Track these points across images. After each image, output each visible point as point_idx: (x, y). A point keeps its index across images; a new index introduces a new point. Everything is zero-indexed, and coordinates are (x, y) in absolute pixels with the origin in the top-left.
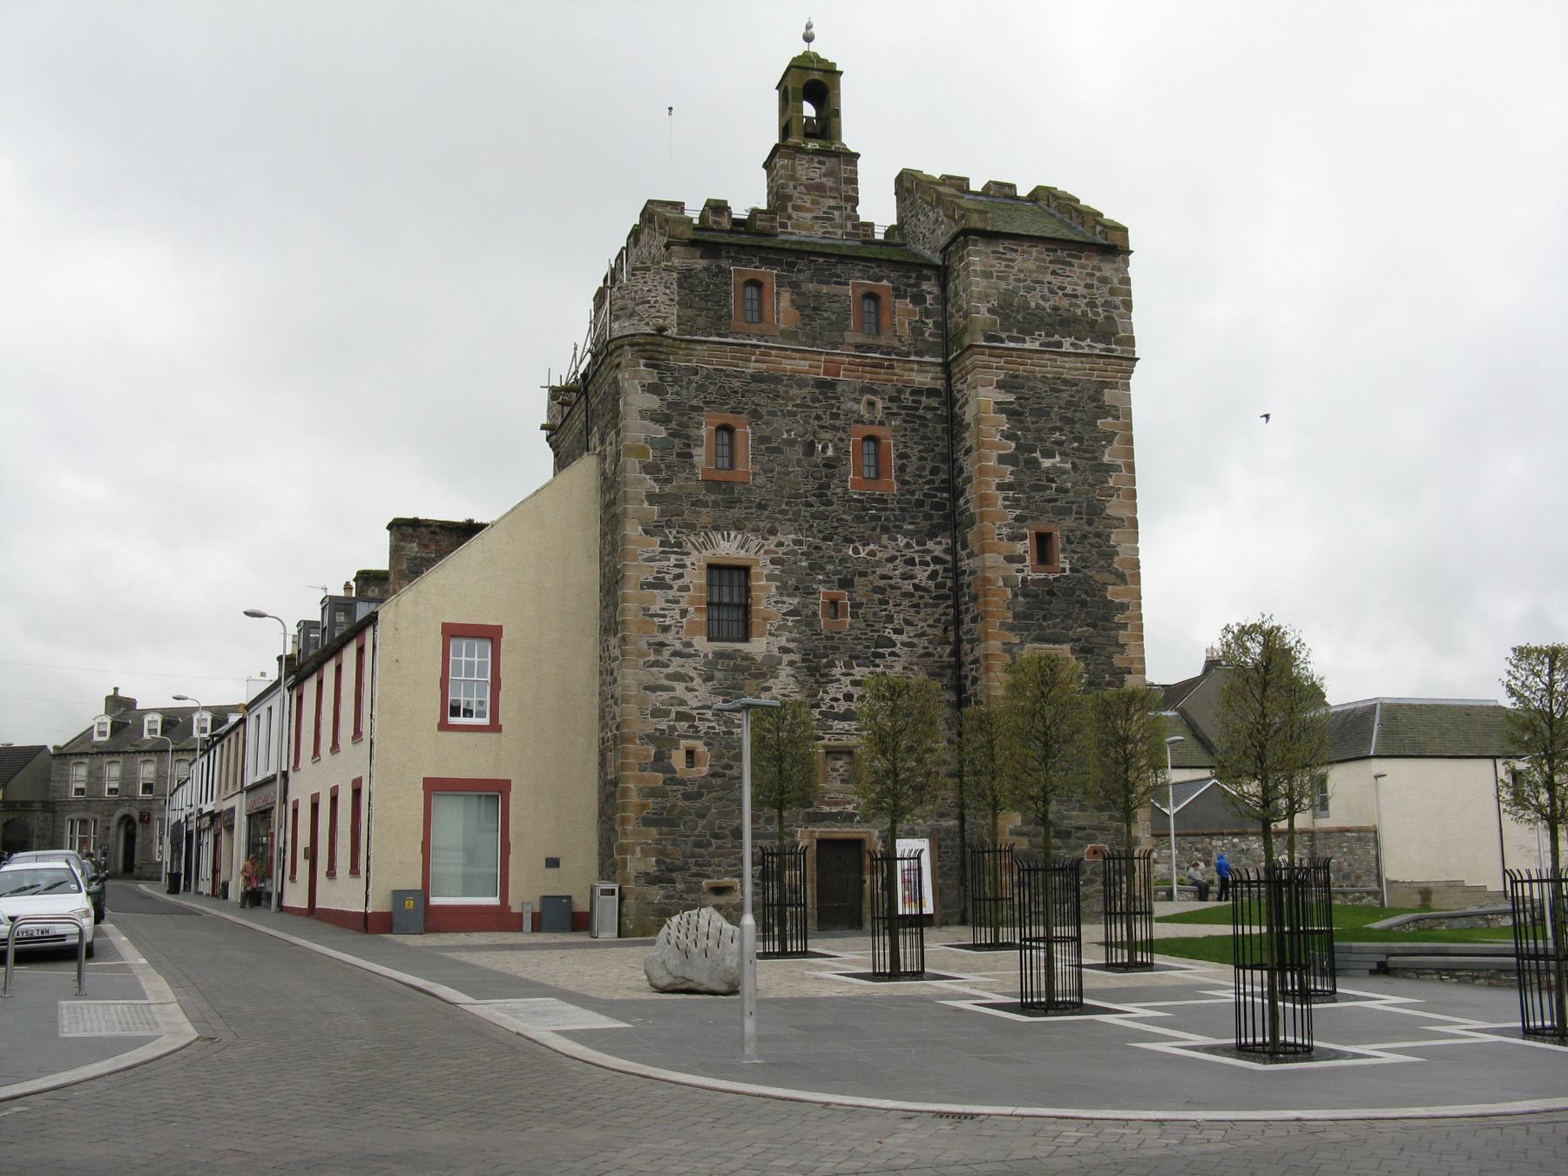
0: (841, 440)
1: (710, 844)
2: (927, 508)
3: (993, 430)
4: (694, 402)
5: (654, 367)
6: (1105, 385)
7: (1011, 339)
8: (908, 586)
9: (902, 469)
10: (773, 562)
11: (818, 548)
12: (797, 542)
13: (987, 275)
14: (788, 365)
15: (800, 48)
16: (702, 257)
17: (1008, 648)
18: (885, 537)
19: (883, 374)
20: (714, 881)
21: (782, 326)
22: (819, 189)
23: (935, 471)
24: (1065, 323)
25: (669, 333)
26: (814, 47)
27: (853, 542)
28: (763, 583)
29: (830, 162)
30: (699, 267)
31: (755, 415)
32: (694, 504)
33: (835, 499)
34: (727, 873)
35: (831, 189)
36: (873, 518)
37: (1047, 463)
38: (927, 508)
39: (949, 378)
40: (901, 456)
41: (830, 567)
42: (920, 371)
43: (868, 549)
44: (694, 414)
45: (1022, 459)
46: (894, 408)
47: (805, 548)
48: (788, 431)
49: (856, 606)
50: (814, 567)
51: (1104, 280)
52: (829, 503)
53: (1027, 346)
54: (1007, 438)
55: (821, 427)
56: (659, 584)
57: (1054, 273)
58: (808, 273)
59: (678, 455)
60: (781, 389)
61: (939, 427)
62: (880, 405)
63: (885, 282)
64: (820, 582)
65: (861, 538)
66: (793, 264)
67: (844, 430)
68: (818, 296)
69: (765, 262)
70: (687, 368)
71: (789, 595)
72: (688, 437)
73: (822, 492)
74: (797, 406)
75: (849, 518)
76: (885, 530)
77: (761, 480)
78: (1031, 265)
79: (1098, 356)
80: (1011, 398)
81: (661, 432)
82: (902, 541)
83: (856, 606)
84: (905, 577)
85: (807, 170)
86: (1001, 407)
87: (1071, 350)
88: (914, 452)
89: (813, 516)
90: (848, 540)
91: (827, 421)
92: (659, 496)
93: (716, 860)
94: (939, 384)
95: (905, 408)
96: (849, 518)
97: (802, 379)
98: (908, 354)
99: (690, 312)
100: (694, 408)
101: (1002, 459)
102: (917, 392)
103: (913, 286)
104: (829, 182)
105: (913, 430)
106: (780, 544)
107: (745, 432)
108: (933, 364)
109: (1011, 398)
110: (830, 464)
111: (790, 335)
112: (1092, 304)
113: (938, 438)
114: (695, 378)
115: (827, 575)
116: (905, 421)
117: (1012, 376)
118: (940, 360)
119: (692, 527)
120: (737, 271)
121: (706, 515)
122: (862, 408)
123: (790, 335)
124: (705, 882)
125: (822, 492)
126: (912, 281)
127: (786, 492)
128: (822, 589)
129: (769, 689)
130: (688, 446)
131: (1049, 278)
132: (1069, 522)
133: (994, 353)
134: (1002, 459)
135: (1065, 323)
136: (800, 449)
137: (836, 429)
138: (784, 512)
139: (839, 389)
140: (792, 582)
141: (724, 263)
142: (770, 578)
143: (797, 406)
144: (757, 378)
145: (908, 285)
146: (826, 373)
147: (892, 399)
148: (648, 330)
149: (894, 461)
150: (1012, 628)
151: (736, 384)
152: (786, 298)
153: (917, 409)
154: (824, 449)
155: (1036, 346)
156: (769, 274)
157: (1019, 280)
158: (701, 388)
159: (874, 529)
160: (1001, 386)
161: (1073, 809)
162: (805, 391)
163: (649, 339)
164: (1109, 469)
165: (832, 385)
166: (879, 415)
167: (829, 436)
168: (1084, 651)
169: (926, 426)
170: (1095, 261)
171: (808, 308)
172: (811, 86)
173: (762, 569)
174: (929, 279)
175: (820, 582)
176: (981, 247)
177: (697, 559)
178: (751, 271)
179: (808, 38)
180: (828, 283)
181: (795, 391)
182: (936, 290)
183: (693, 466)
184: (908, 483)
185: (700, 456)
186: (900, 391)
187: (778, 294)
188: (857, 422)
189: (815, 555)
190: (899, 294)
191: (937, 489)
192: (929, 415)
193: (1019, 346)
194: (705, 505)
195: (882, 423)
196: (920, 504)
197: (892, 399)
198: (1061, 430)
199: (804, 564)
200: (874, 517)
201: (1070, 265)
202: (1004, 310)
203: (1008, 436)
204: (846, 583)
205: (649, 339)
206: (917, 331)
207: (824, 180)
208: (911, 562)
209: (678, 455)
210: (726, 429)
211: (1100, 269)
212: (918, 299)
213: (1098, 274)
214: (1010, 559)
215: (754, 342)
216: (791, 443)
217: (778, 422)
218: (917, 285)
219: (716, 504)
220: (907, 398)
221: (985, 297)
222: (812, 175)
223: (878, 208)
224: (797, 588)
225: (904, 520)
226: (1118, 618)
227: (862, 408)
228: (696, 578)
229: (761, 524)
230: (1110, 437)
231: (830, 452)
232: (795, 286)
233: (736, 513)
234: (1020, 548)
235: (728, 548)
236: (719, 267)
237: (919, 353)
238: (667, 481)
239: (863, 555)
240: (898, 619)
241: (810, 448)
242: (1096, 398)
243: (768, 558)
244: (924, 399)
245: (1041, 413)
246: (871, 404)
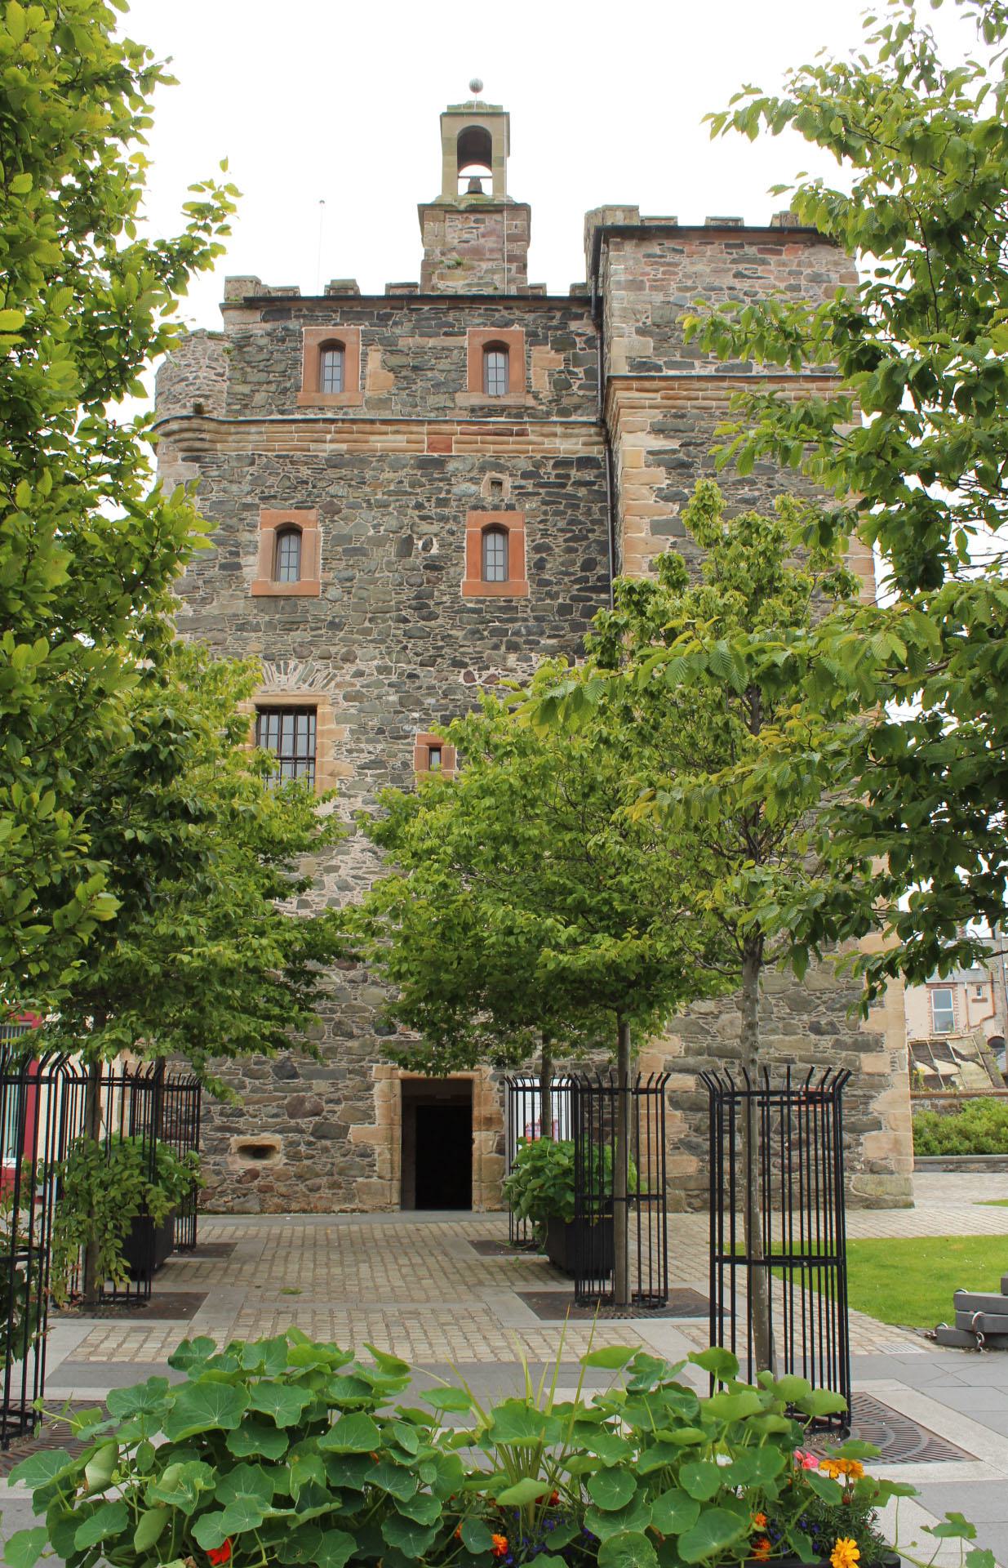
0: (452, 533)
1: (242, 1086)
2: (576, 615)
3: (645, 490)
4: (249, 500)
5: (196, 459)
7: (672, 365)
9: (540, 565)
10: (346, 698)
11: (412, 676)
12: (381, 670)
13: (635, 285)
14: (378, 443)
15: (463, 97)
16: (264, 320)
18: (512, 659)
19: (511, 444)
20: (248, 1139)
21: (368, 394)
23: (589, 565)
25: (214, 415)
26: (487, 98)
27: (464, 665)
28: (333, 726)
29: (490, 221)
30: (260, 332)
31: (331, 511)
32: (241, 628)
33: (439, 610)
34: (264, 1128)
35: (492, 250)
36: (495, 632)
38: (576, 615)
39: (608, 440)
40: (538, 549)
41: (432, 701)
42: (565, 436)
43: (486, 674)
44: (245, 514)
46: (529, 485)
47: (394, 678)
48: (374, 527)
51: (816, 279)
52: (432, 616)
53: (698, 371)
54: (666, 499)
55: (422, 518)
57: (738, 275)
58: (411, 325)
59: (223, 567)
60: (368, 474)
61: (596, 508)
62: (508, 482)
63: (516, 327)
64: (415, 721)
65: (478, 659)
66: (389, 316)
67: (455, 518)
68: (420, 352)
70: (239, 458)
71: (368, 741)
72: (238, 545)
73: (421, 606)
74: (389, 493)
75: (460, 634)
76: (513, 647)
77: (333, 592)
78: (700, 267)
79: (806, 378)
80: (674, 444)
82: (538, 660)
85: (455, 231)
87: (766, 373)
88: (558, 543)
89: (409, 635)
90: (458, 664)
91: (432, 510)
92: (192, 620)
93: (251, 1108)
94: (596, 451)
95: (543, 485)
96: (460, 634)
97: (397, 459)
98: (548, 414)
99: (246, 389)
100: (247, 507)
102: (559, 464)
103: (556, 328)
104: (490, 243)
105: (556, 513)
106: (359, 674)
107: (314, 529)
108: (584, 424)
109: (674, 444)
110: (433, 566)
113: (593, 522)
114: (251, 469)
115: (426, 711)
116: (545, 503)
117: (675, 416)
118: (593, 419)
120: (314, 333)
121: (255, 643)
122: (483, 490)
123: (383, 403)
124: (235, 1140)
125: (421, 606)
126: (555, 323)
127: (373, 605)
128: (417, 730)
129: (336, 869)
130: (237, 554)
131: (729, 280)
134: (657, 528)
136: (392, 549)
137: (443, 519)
138: (366, 632)
139: (451, 466)
140: (374, 723)
141: (293, 324)
142: (341, 719)
143: (389, 493)
145: (549, 328)
146: (431, 448)
147: (526, 475)
148: (185, 413)
149: (528, 557)
151: (305, 472)
152: (375, 357)
153: (563, 486)
154: (427, 547)
155: (710, 370)
156: (351, 332)
157: (687, 289)
158: (256, 481)
159: (496, 647)
160: (658, 430)
161: (774, 1031)
162: (402, 473)
163: (185, 424)
165: (440, 463)
166: (507, 494)
167: (435, 528)
169: (576, 507)
170: (804, 254)
171: (408, 372)
174: (579, 317)
175: (415, 721)
176: (629, 248)
178: (327, 331)
179: (476, 88)
180: (437, 335)
181: (388, 475)
182: (590, 331)
183: (240, 580)
184: (548, 583)
185: (253, 567)
186: (538, 465)
187: (365, 354)
188: (475, 508)
189: (409, 685)
190: (533, 338)
191: (594, 589)
192: (582, 492)
193: (685, 373)
194: (256, 629)
195: (510, 507)
196: (564, 610)
197: (526, 475)
198: (752, 483)
199: (393, 698)
200: (500, 627)
201: (764, 262)
205: (185, 424)
206: (561, 385)
207: (482, 240)
209: (223, 567)
211: (811, 265)
212: (563, 344)
213: (809, 271)
215: (330, 415)
216: (379, 542)
217: (365, 516)
218: (563, 325)
219: (270, 625)
220: (549, 472)
221: (631, 313)
222: (466, 236)
223: (556, 264)
224: (381, 731)
225: (542, 633)
227: (483, 490)
229: (333, 650)
231: (435, 551)
233: (297, 636)
236: (286, 329)
237: (564, 412)
238: (204, 601)
239: (479, 682)
241: (406, 546)
243: (340, 694)
244: (573, 472)
246: (497, 484)
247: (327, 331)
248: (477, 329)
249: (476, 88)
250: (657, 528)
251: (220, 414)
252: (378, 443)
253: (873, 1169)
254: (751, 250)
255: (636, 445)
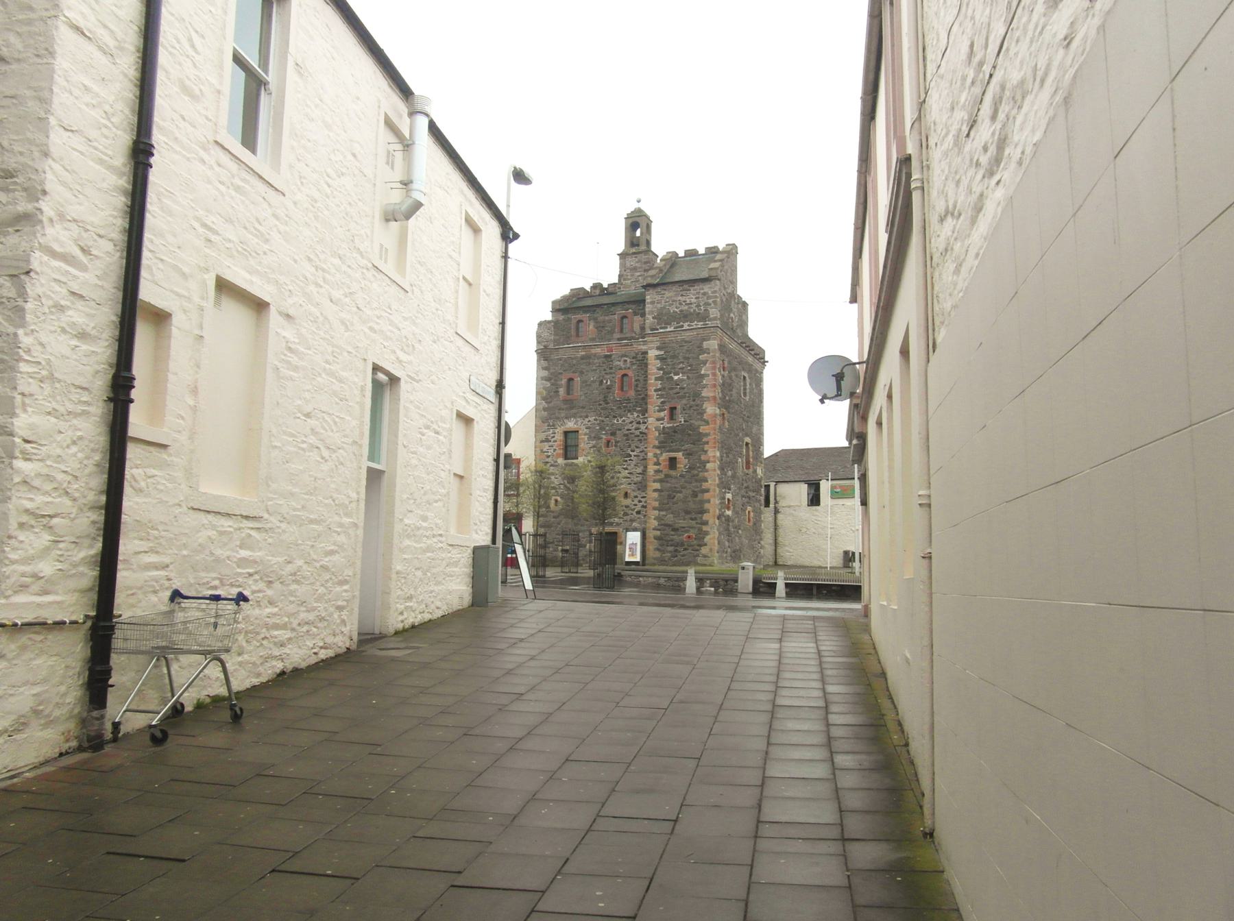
6: (704, 340)
8: (637, 433)
13: (653, 303)
14: (593, 351)
17: (656, 455)
19: (629, 348)
22: (635, 269)
24: (686, 316)
37: (676, 378)
45: (665, 377)
49: (617, 442)
50: (602, 429)
51: (704, 294)
56: (547, 440)
69: (585, 312)
81: (548, 384)
83: (617, 442)
84: (637, 429)
85: (631, 262)
86: (657, 357)
101: (657, 379)
110: (609, 388)
111: (593, 340)
112: (698, 306)
119: (558, 418)
120: (575, 317)
123: (593, 340)
132: (684, 401)
133: (654, 335)
135: (686, 316)
144: (583, 358)
149: (634, 383)
150: (658, 448)
160: (658, 348)
164: (703, 376)
165: (610, 356)
168: (688, 454)
171: (600, 327)
172: (637, 223)
173: (583, 430)
177: (559, 431)
178: (579, 317)
190: (635, 314)
202: (658, 317)
203: (659, 369)
204: (613, 434)
208: (639, 423)
210: (571, 380)
214: (658, 420)
226: (705, 440)
227: (621, 364)
228: (559, 437)
230: (705, 363)
232: (595, 319)
233: (574, 411)
234: (662, 414)
235: (571, 425)
240: (633, 446)
242: (700, 347)
245: (674, 357)
247: (579, 317)
248: (620, 312)
249: (639, 201)
250: (657, 379)
251: (551, 346)
252: (593, 351)
253: (705, 556)
254: (686, 286)
255: (652, 353)
